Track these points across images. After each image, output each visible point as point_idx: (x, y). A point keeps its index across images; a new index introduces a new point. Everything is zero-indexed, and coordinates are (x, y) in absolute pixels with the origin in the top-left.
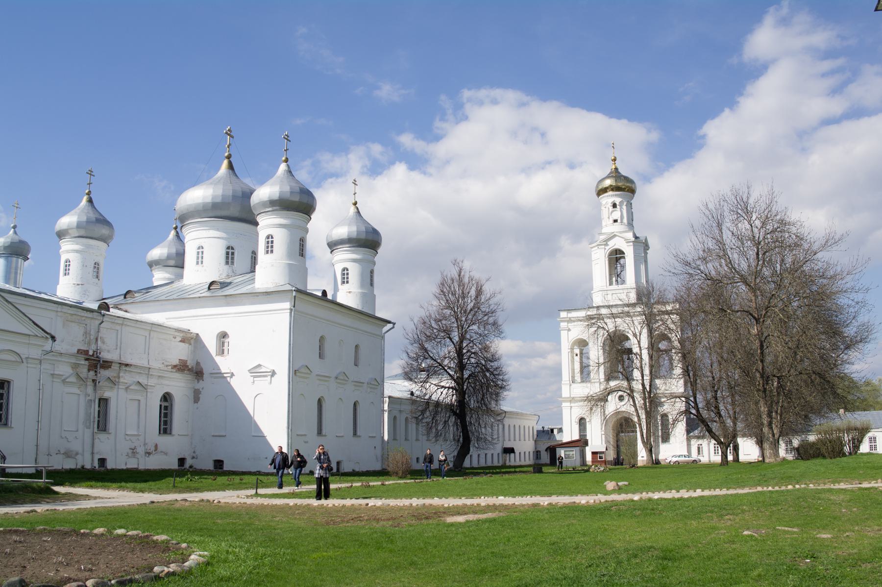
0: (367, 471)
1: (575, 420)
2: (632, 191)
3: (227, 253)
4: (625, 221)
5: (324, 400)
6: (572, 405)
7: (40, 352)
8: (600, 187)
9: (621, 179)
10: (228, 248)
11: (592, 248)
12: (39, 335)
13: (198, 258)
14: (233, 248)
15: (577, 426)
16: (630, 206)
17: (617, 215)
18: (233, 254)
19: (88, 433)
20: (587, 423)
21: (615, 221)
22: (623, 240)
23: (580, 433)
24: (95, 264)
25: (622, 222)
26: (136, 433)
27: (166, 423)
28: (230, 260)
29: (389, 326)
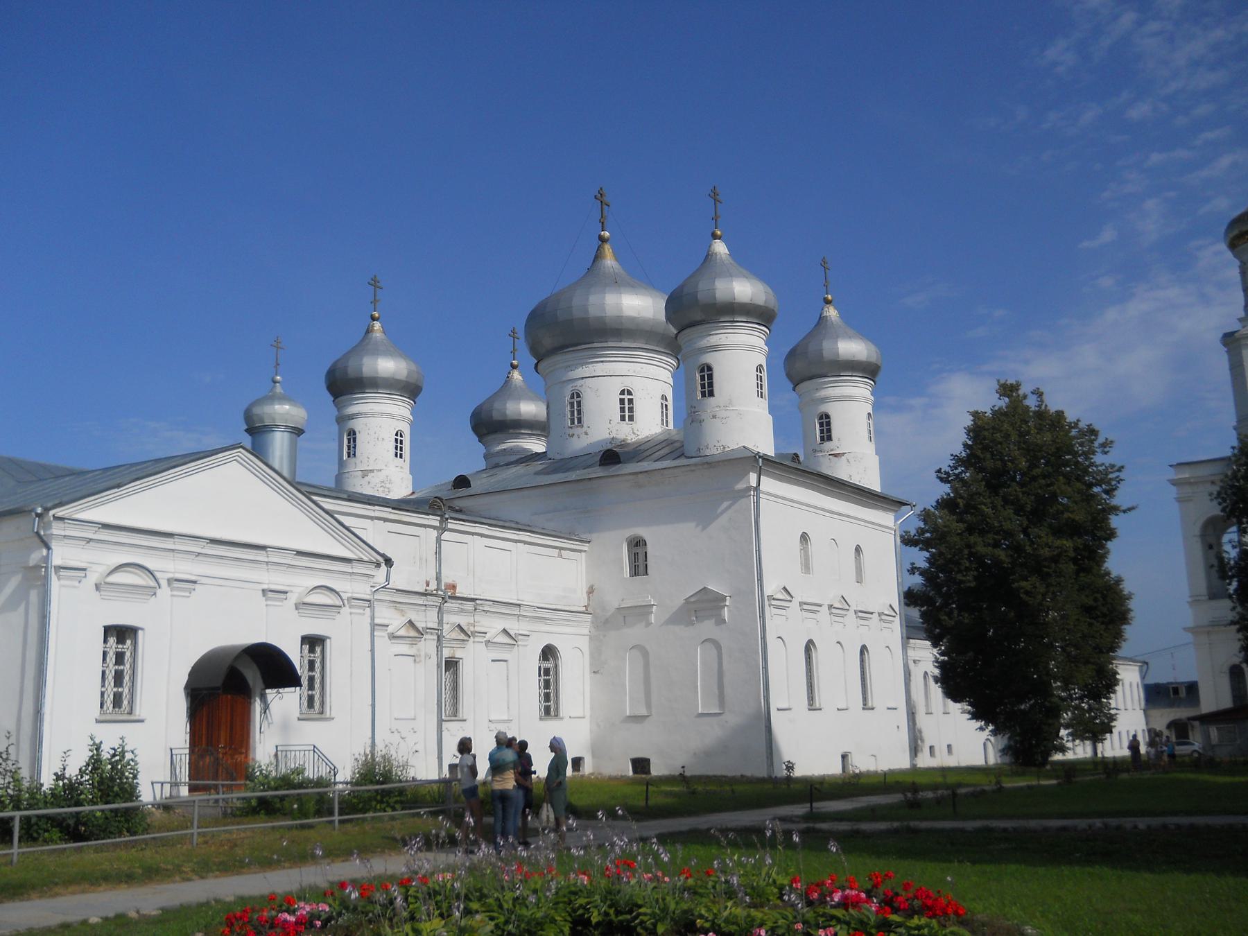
3: (622, 401)
5: (814, 645)
7: (368, 590)
10: (622, 392)
12: (366, 559)
14: (629, 393)
18: (631, 401)
24: (397, 435)
26: (505, 717)
27: (547, 697)
28: (627, 414)
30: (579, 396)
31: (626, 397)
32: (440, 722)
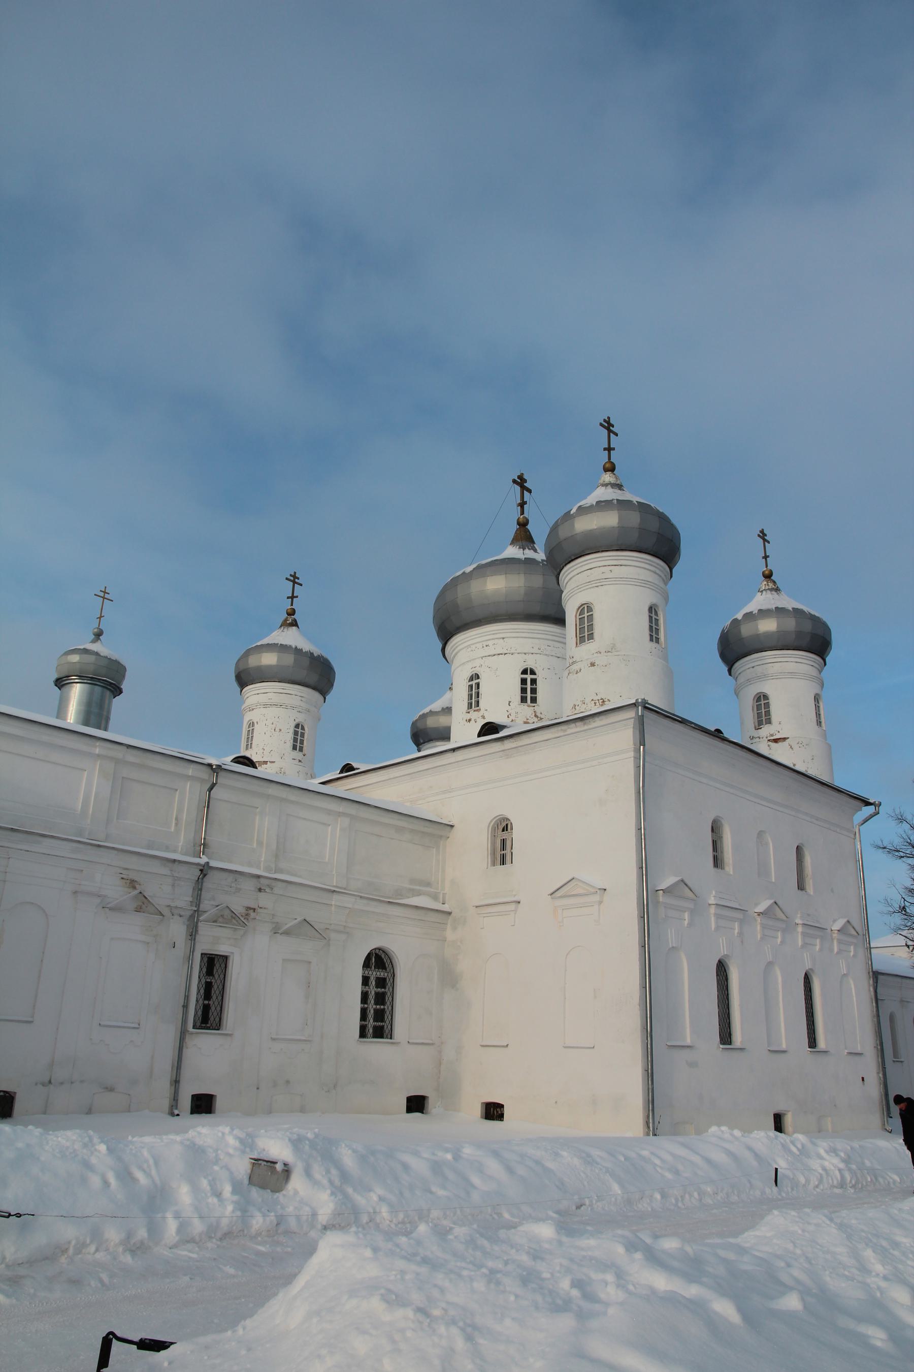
3: (524, 681)
10: (525, 672)
13: (470, 697)
14: (533, 672)
18: (534, 681)
19: (170, 1034)
24: (297, 726)
28: (529, 695)
29: (870, 810)
30: (478, 677)
31: (529, 677)
32: (183, 1035)
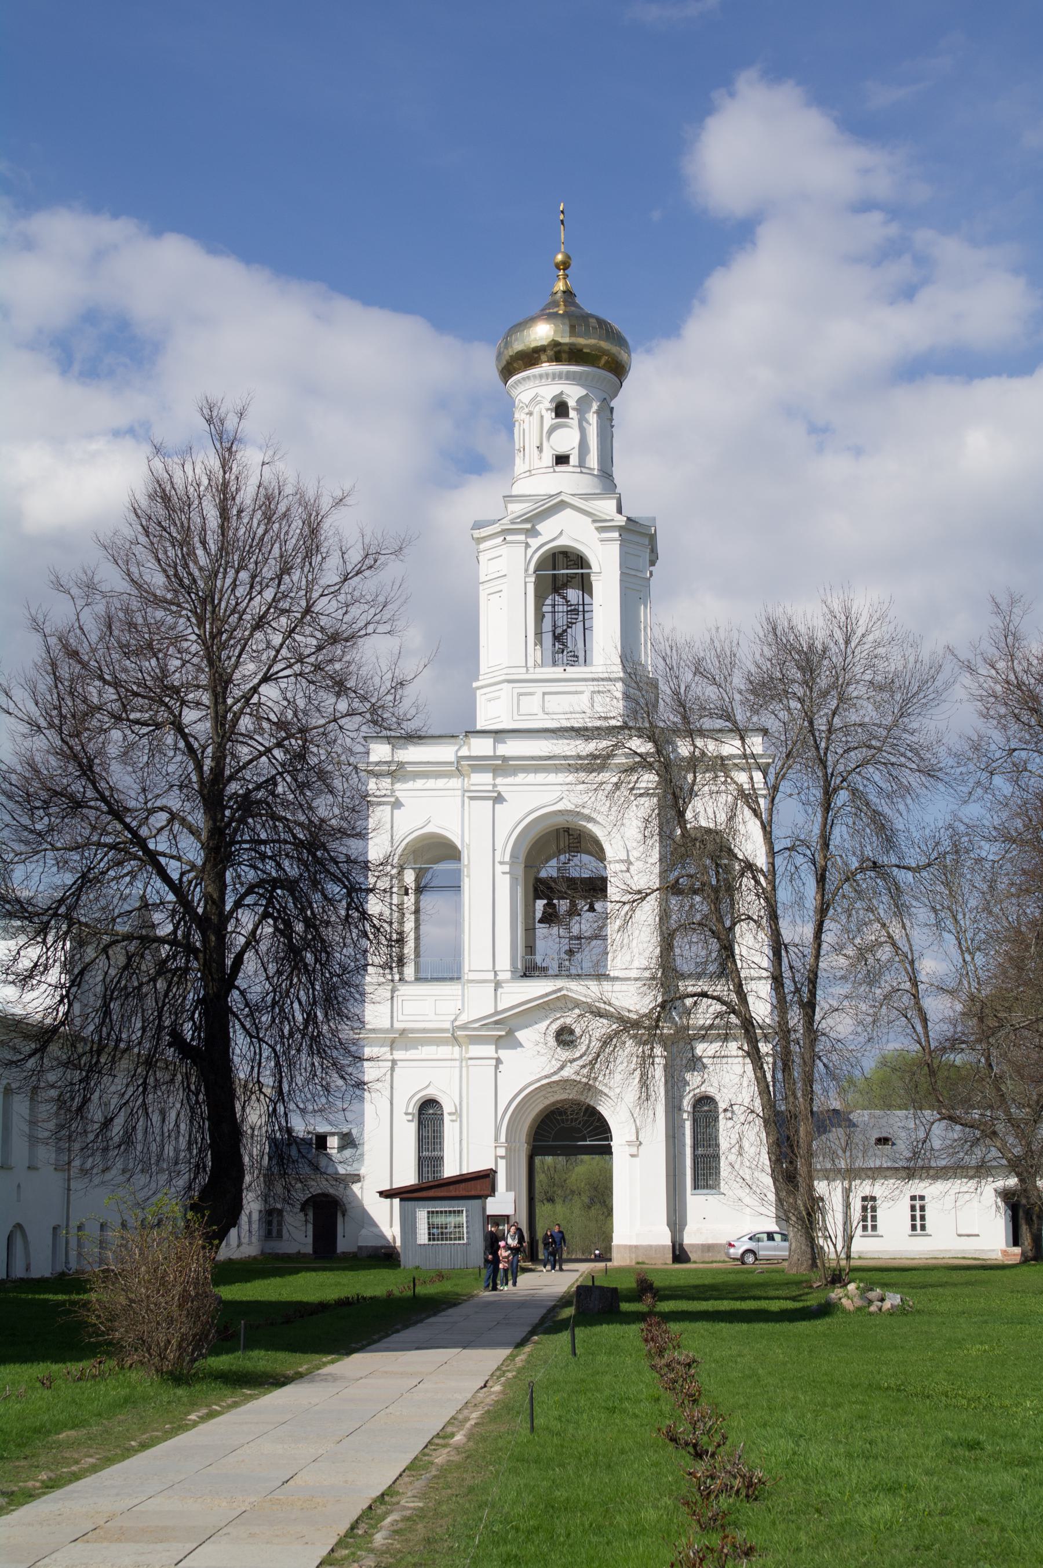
0: (299, 1253)
1: (406, 1103)
2: (618, 370)
4: (593, 461)
6: (398, 1055)
8: (518, 346)
9: (587, 325)
11: (479, 540)
15: (413, 1127)
16: (606, 414)
17: (567, 440)
20: (447, 1118)
21: (562, 460)
22: (590, 520)
23: (420, 1149)
25: (582, 464)
